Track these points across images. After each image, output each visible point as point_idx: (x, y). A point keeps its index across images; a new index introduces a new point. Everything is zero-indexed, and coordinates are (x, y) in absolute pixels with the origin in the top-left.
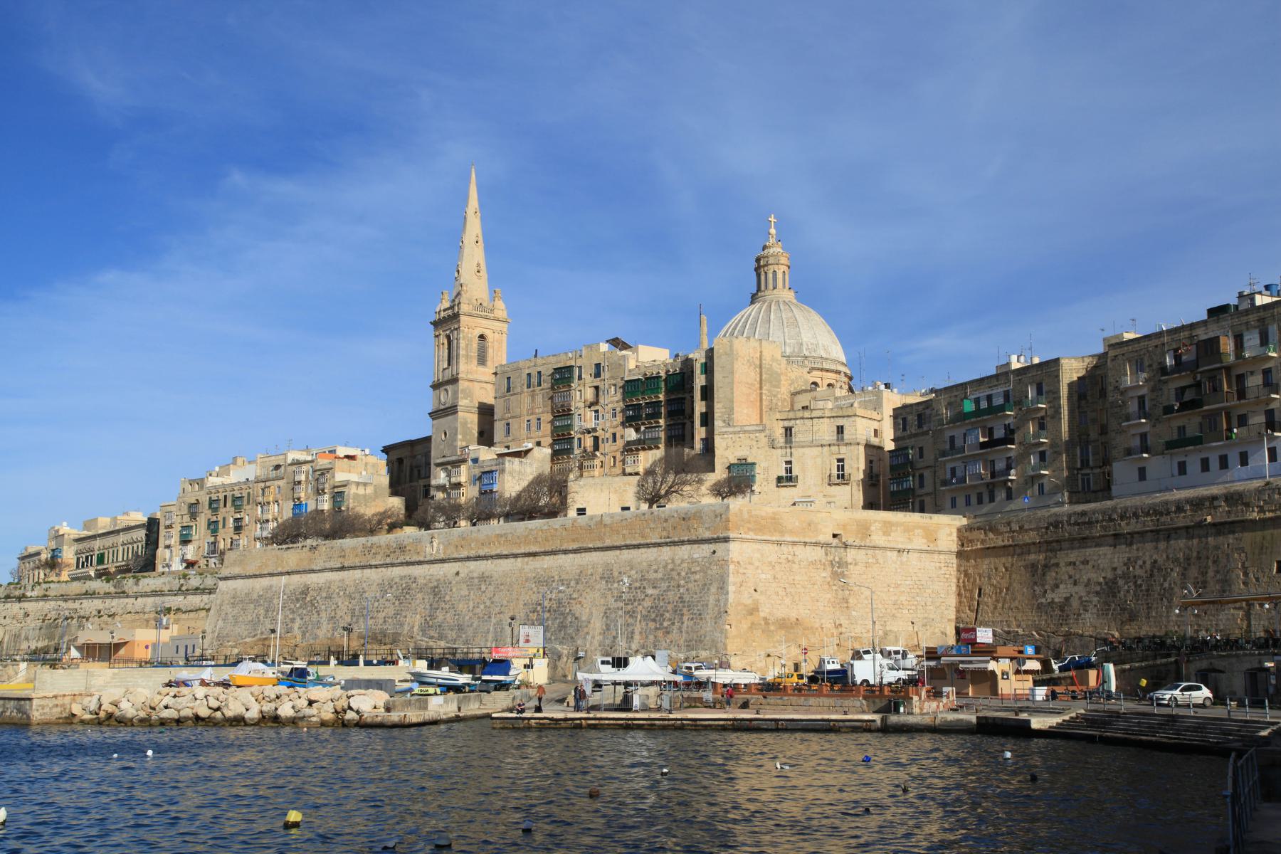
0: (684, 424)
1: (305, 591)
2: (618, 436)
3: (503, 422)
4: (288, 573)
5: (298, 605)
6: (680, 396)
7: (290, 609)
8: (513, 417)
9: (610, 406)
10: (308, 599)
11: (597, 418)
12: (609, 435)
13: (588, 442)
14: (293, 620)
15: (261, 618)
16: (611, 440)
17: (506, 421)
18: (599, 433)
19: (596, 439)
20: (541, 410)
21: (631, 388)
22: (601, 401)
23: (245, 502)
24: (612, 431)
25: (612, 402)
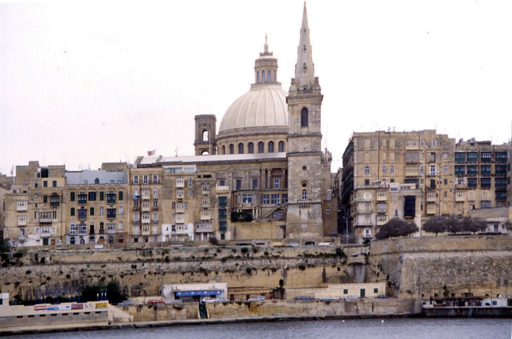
0: (490, 178)
1: (490, 260)
2: (448, 181)
3: (363, 165)
4: (472, 251)
5: (486, 268)
6: (488, 164)
7: (481, 270)
8: (372, 163)
9: (443, 164)
10: (494, 264)
11: (433, 170)
12: (442, 180)
13: (428, 183)
14: (486, 275)
15: (455, 274)
16: (443, 183)
17: (366, 165)
18: (437, 179)
19: (433, 182)
20: (394, 162)
21: (459, 157)
22: (436, 162)
23: (118, 198)
24: (444, 178)
25: (445, 162)
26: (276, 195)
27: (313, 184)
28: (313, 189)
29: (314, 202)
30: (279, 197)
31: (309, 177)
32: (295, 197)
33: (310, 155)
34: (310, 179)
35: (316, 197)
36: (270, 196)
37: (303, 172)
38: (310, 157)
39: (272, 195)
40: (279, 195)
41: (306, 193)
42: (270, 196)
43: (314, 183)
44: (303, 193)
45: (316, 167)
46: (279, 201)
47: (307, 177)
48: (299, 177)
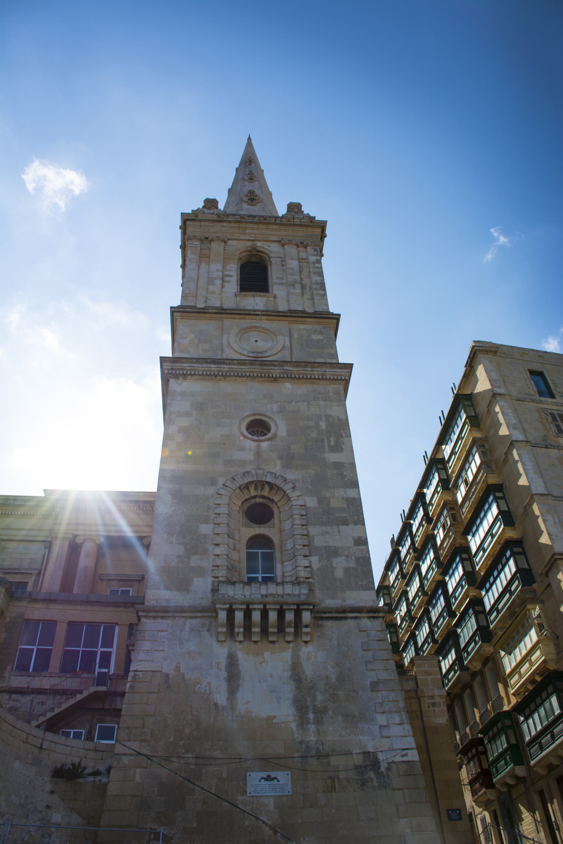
26: (93, 626)
27: (311, 502)
28: (314, 530)
29: (330, 603)
30: (108, 642)
31: (286, 466)
32: (200, 572)
33: (291, 378)
34: (290, 475)
35: (339, 574)
36: (61, 632)
37: (250, 444)
38: (288, 385)
39: (74, 627)
40: (110, 628)
41: (269, 558)
42: (61, 632)
43: (322, 500)
44: (251, 557)
45: (323, 425)
46: (106, 659)
47: (277, 468)
48: (229, 462)
